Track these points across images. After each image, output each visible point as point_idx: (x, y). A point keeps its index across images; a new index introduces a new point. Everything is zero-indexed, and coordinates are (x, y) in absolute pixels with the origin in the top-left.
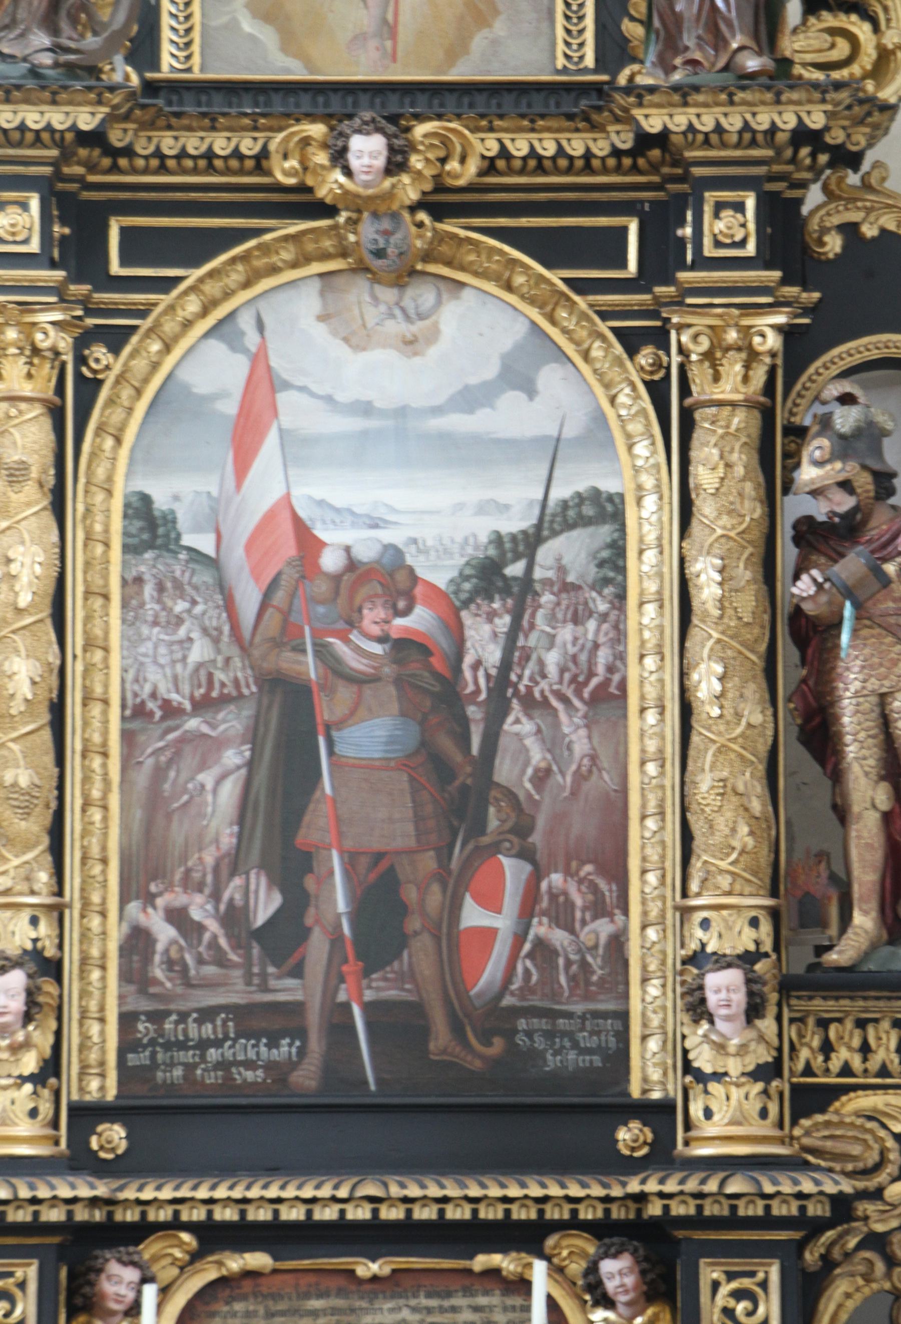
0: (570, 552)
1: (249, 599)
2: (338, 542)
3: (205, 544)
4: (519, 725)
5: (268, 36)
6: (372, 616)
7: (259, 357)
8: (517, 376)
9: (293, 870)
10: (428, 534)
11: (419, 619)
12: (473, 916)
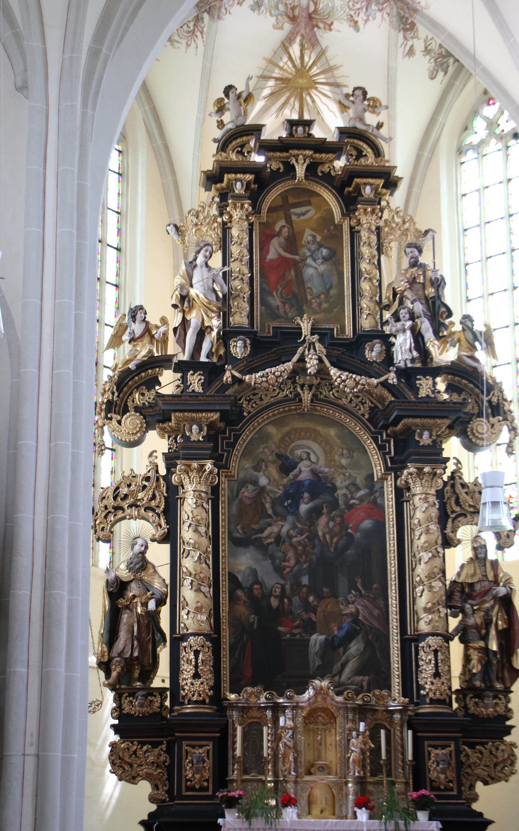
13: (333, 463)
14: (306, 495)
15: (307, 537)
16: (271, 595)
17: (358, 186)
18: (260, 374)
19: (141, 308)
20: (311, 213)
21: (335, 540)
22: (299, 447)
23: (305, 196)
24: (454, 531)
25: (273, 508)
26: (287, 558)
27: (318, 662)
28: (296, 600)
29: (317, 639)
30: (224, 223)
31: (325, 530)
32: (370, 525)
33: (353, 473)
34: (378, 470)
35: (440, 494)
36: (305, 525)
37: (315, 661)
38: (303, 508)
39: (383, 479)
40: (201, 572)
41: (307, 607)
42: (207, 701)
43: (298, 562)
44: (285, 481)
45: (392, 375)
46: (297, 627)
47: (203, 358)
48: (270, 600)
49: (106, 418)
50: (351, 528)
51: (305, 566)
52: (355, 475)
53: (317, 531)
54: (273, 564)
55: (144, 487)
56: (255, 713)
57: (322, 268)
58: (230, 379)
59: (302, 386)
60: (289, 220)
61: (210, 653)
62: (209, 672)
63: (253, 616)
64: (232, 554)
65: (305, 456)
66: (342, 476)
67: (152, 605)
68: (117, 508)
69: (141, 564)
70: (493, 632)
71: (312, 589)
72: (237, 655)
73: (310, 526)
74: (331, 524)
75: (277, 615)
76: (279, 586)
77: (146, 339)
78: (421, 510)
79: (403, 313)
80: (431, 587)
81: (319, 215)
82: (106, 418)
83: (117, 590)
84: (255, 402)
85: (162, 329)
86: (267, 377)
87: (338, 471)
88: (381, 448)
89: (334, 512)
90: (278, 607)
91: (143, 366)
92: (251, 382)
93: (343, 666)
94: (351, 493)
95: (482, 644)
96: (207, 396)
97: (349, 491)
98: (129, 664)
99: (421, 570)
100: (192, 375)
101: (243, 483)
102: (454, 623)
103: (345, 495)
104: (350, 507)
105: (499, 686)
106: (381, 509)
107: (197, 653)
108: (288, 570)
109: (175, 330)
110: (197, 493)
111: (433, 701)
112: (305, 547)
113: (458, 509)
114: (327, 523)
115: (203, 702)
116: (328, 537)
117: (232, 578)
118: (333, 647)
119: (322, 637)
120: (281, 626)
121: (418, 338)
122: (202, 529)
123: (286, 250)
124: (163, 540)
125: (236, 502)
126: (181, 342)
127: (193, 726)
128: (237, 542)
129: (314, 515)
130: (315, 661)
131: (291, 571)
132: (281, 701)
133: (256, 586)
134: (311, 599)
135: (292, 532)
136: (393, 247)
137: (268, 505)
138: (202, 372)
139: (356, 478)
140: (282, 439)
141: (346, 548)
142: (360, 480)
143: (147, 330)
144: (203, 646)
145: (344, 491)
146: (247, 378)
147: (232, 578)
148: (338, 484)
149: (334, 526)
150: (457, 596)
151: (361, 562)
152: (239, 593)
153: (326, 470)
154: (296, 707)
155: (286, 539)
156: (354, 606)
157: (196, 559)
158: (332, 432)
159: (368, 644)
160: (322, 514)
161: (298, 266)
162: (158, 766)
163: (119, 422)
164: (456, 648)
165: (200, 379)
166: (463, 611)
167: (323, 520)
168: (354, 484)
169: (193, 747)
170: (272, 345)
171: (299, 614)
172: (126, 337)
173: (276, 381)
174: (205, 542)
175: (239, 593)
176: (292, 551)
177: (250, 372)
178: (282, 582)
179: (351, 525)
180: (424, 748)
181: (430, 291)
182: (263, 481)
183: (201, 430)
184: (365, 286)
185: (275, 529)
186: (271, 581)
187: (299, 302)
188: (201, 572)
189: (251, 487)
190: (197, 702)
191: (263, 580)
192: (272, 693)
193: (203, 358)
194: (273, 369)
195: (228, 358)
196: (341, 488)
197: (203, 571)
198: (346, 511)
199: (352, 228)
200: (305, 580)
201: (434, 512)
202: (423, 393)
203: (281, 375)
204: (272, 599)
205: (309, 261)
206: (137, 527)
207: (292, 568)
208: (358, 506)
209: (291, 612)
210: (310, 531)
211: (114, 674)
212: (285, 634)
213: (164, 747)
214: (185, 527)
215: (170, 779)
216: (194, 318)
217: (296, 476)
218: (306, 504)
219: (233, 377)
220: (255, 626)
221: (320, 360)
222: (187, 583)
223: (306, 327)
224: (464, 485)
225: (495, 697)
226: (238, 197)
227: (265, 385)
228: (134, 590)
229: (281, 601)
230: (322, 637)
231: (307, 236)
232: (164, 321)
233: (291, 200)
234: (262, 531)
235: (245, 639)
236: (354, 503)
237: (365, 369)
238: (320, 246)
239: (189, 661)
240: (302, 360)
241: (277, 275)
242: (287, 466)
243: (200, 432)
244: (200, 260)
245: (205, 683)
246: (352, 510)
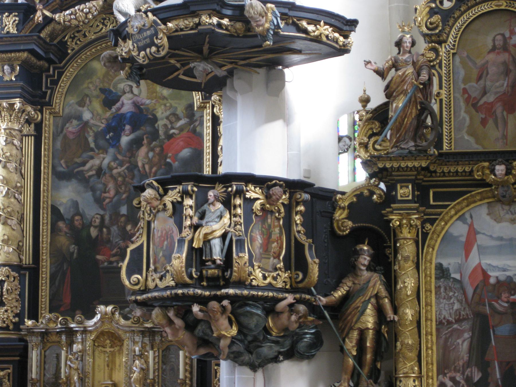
2: (493, 274)
3: (457, 276)
5: (472, 140)
6: (504, 296)
9: (484, 367)
13: (155, 94)
14: (128, 127)
15: (127, 168)
16: (90, 225)
21: (154, 169)
25: (95, 141)
26: (107, 189)
28: (114, 229)
31: (145, 160)
32: (188, 154)
36: (125, 156)
38: (125, 140)
40: (8, 207)
42: (11, 327)
43: (117, 193)
44: (108, 114)
46: (114, 255)
48: (89, 230)
50: (170, 157)
51: (124, 196)
52: (176, 105)
53: (137, 162)
54: (94, 195)
56: (54, 338)
58: (41, 19)
61: (16, 282)
62: (14, 300)
63: (73, 246)
64: (55, 188)
65: (128, 89)
66: (163, 107)
72: (57, 283)
73: (130, 158)
74: (151, 154)
76: (99, 216)
84: (79, 39)
86: (75, 15)
87: (159, 102)
89: (154, 143)
90: (97, 237)
92: (60, 20)
94: (171, 123)
96: (21, 36)
97: (170, 121)
100: (8, 16)
101: (68, 119)
103: (165, 125)
104: (170, 137)
106: (200, 136)
108: (107, 200)
110: (7, 131)
112: (124, 178)
114: (147, 153)
115: (7, 328)
116: (147, 167)
117: (55, 211)
120: (99, 254)
125: (60, 138)
129: (134, 146)
131: (111, 202)
132: (72, 326)
133: (77, 218)
135: (112, 164)
137: (91, 139)
138: (16, 14)
139: (176, 108)
142: (180, 110)
144: (8, 276)
145: (165, 121)
146: (57, 16)
147: (55, 211)
148: (159, 115)
149: (154, 156)
152: (61, 224)
153: (148, 102)
154: (85, 331)
155: (107, 171)
157: (4, 193)
160: (142, 145)
165: (15, 20)
167: (143, 151)
168: (174, 114)
171: (117, 242)
173: (86, 18)
175: (61, 224)
176: (112, 182)
178: (102, 212)
179: (170, 155)
180: (211, 366)
182: (87, 116)
183: (13, 69)
185: (96, 162)
186: (91, 211)
188: (8, 207)
189: (75, 122)
191: (83, 211)
192: (67, 319)
194: (82, 6)
196: (162, 119)
197: (11, 205)
198: (166, 141)
203: (90, 12)
204: (92, 229)
207: (112, 198)
208: (178, 136)
209: (109, 241)
210: (130, 162)
212: (103, 262)
217: (119, 109)
218: (127, 136)
219: (45, 17)
220: (75, 255)
227: (74, 22)
229: (101, 231)
234: (84, 164)
235: (65, 268)
236: (174, 133)
243: (11, 72)
245: (9, 311)
246: (171, 141)
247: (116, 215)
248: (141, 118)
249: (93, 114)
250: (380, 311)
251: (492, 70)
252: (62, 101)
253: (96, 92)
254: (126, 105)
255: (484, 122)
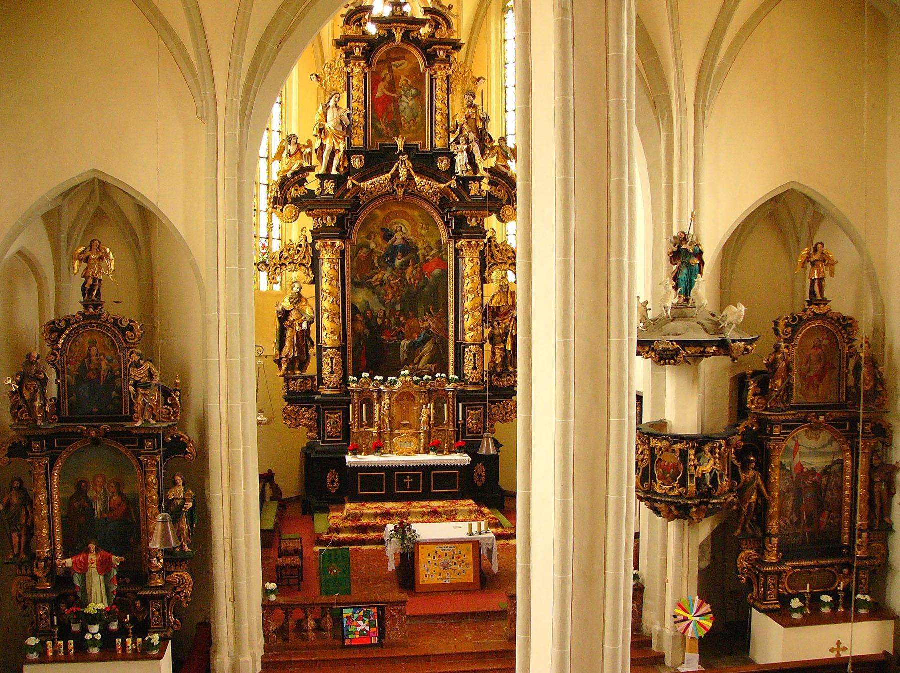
0: (836, 467)
1: (795, 476)
4: (829, 493)
6: (810, 478)
7: (797, 442)
8: (830, 443)
9: (799, 515)
10: (818, 466)
11: (816, 478)
12: (822, 519)
17: (435, 50)
18: (370, 182)
19: (295, 135)
20: (406, 65)
22: (395, 223)
23: (400, 54)
24: (490, 274)
27: (406, 357)
28: (393, 319)
29: (405, 343)
30: (349, 73)
33: (429, 239)
34: (444, 238)
35: (482, 253)
37: (403, 356)
38: (398, 262)
39: (448, 242)
41: (400, 324)
43: (394, 296)
45: (454, 181)
47: (334, 172)
49: (274, 208)
55: (299, 251)
57: (411, 102)
59: (398, 186)
60: (391, 70)
65: (399, 229)
67: (305, 326)
68: (281, 265)
69: (299, 298)
70: (509, 339)
71: (403, 312)
74: (415, 272)
75: (381, 329)
77: (299, 156)
78: (469, 266)
79: (462, 139)
80: (473, 315)
81: (410, 66)
82: (274, 208)
83: (284, 315)
85: (308, 150)
88: (446, 223)
91: (295, 174)
93: (421, 359)
95: (503, 346)
98: (292, 361)
99: (468, 305)
101: (360, 247)
102: (487, 332)
104: (427, 261)
105: (511, 369)
107: (332, 359)
109: (316, 150)
111: (471, 383)
113: (493, 262)
115: (337, 387)
117: (354, 307)
118: (415, 348)
119: (408, 342)
121: (471, 155)
122: (334, 283)
123: (388, 90)
124: (312, 282)
126: (320, 158)
127: (329, 403)
128: (355, 284)
130: (403, 356)
134: (402, 319)
136: (458, 88)
137: (375, 261)
140: (385, 218)
141: (424, 287)
143: (299, 149)
146: (362, 184)
147: (354, 307)
148: (419, 246)
150: (489, 314)
151: (434, 295)
154: (391, 392)
156: (428, 322)
158: (416, 213)
159: (435, 344)
161: (396, 101)
162: (312, 420)
163: (282, 210)
164: (488, 347)
166: (492, 325)
167: (410, 269)
168: (430, 247)
169: (331, 413)
170: (378, 158)
172: (284, 155)
174: (336, 290)
175: (358, 316)
177: (364, 181)
181: (480, 125)
182: (373, 246)
183: (333, 219)
184: (439, 117)
186: (378, 308)
187: (396, 127)
189: (365, 249)
190: (333, 388)
193: (334, 172)
194: (379, 179)
195: (350, 170)
199: (432, 76)
200: (398, 308)
201: (478, 268)
202: (473, 193)
205: (404, 97)
206: (296, 275)
209: (389, 327)
211: (284, 368)
213: (315, 408)
214: (324, 280)
215: (319, 426)
216: (328, 143)
219: (354, 184)
221: (409, 170)
222: (326, 316)
223: (400, 144)
224: (496, 246)
225: (509, 375)
226: (357, 58)
228: (294, 316)
229: (384, 320)
230: (408, 342)
231: (402, 81)
232: (310, 144)
233: (393, 56)
237: (437, 176)
238: (411, 87)
239: (327, 364)
240: (397, 169)
241: (382, 109)
242: (388, 235)
244: (332, 103)
247: (393, 311)
248: (408, 248)
249: (377, 244)
250: (760, 494)
251: (813, 358)
252: (357, 236)
253: (379, 230)
254: (398, 239)
255: (808, 388)
